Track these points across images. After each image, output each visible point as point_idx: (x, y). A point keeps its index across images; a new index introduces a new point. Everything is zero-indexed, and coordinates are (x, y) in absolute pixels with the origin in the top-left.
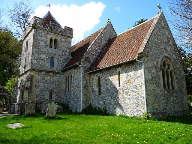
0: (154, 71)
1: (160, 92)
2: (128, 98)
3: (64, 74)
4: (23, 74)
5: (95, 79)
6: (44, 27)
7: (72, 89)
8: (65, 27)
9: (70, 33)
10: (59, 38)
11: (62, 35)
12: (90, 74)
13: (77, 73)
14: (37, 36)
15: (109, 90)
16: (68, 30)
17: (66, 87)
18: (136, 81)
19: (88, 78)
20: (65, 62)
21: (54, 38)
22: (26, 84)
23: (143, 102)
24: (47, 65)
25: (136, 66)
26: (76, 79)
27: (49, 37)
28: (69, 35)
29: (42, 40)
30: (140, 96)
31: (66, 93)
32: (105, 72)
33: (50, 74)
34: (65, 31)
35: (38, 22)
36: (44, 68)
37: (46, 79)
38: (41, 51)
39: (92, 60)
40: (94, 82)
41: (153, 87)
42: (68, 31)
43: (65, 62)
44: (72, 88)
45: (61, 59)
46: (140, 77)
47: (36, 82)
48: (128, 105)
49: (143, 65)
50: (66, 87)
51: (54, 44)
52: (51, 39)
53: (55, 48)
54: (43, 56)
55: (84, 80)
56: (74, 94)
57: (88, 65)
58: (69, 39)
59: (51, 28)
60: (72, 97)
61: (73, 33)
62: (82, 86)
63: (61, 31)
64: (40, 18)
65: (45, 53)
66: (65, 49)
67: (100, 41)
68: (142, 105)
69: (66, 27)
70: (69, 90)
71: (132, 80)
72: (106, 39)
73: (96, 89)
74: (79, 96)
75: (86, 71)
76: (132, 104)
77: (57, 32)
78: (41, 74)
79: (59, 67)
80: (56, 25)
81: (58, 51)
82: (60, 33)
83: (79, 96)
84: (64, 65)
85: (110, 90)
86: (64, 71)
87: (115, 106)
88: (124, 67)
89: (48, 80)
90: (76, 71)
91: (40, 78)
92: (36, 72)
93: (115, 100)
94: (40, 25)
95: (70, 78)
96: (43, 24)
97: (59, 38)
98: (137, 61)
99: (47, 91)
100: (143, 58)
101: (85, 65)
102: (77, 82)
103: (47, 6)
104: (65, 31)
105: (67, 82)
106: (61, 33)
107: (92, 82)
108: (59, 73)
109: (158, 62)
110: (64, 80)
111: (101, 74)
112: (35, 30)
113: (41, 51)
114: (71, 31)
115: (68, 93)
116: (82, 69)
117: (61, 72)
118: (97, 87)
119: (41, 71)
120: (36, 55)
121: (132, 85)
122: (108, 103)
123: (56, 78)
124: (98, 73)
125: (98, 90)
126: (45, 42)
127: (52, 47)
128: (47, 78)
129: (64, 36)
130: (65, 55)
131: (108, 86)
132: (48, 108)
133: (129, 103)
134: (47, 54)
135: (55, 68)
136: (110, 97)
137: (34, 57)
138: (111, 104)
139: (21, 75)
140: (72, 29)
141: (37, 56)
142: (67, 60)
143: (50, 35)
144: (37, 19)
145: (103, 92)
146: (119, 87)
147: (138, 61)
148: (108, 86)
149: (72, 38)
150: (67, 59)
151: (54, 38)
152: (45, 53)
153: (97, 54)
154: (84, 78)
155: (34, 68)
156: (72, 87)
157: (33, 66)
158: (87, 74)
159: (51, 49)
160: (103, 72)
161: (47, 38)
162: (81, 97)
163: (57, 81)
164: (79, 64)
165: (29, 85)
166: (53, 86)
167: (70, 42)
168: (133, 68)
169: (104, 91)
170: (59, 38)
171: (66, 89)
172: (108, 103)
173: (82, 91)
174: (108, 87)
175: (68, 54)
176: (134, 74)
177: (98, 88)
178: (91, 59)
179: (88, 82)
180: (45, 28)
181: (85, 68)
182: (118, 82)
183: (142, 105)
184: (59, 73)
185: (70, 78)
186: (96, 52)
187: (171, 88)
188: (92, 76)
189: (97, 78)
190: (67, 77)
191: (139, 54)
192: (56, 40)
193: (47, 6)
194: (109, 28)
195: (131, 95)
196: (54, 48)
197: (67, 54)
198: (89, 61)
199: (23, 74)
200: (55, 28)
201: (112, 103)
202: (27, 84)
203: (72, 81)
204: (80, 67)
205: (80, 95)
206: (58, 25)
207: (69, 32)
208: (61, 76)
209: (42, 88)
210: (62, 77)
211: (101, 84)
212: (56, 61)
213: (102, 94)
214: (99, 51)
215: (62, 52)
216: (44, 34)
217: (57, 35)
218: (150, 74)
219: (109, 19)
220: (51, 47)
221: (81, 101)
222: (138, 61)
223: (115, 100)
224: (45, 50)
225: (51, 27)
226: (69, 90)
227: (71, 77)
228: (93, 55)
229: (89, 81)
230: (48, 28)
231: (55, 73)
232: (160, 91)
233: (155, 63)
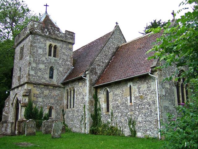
0: (168, 86)
1: (174, 109)
2: (140, 115)
4: (18, 87)
9: (71, 39)
10: (58, 45)
11: (62, 41)
13: (81, 87)
14: (35, 43)
15: (118, 106)
16: (69, 35)
18: (149, 97)
20: (66, 73)
21: (54, 44)
22: (24, 100)
23: (156, 120)
24: (47, 77)
25: (149, 81)
27: (48, 43)
28: (71, 41)
29: (40, 48)
30: (153, 113)
33: (49, 87)
36: (43, 81)
37: (44, 94)
38: (39, 60)
41: (167, 104)
42: (69, 36)
43: (66, 73)
44: (75, 104)
46: (153, 93)
47: (34, 97)
48: (140, 123)
51: (53, 51)
52: (50, 46)
54: (42, 66)
55: (90, 94)
56: (77, 111)
57: (95, 77)
58: (70, 46)
59: (50, 33)
63: (61, 36)
65: (43, 63)
66: (65, 57)
70: (72, 107)
75: (91, 84)
76: (144, 123)
77: (57, 38)
78: (39, 88)
79: (58, 79)
80: (56, 29)
84: (65, 77)
85: (120, 107)
86: (65, 84)
88: (136, 81)
89: (47, 94)
90: (80, 84)
91: (38, 92)
92: (34, 85)
94: (38, 30)
95: (72, 92)
96: (41, 29)
97: (59, 44)
98: (150, 75)
99: (46, 107)
100: (156, 73)
101: (91, 77)
102: (82, 96)
103: (44, 5)
104: (66, 36)
105: (69, 97)
106: (62, 39)
108: (60, 87)
110: (65, 95)
111: (109, 88)
112: (33, 36)
114: (72, 36)
115: (70, 109)
116: (88, 82)
119: (40, 84)
120: (34, 65)
121: (144, 101)
123: (56, 92)
124: (106, 87)
126: (44, 49)
127: (51, 56)
128: (46, 92)
129: (65, 42)
130: (66, 65)
131: (117, 102)
132: (54, 126)
133: (141, 121)
134: (45, 63)
135: (55, 81)
136: (120, 115)
137: (32, 68)
138: (121, 122)
139: (15, 88)
140: (73, 33)
141: (35, 66)
145: (111, 108)
146: (131, 104)
148: (117, 102)
149: (73, 44)
151: (54, 44)
154: (90, 93)
155: (32, 80)
156: (75, 103)
157: (31, 78)
160: (112, 86)
161: (45, 46)
164: (84, 76)
165: (27, 100)
166: (52, 101)
167: (71, 49)
168: (145, 83)
169: (113, 107)
171: (67, 105)
174: (118, 104)
175: (70, 64)
178: (97, 70)
180: (44, 33)
181: (91, 80)
182: (129, 98)
183: (155, 123)
184: (60, 87)
185: (72, 92)
186: (103, 63)
189: (105, 93)
190: (69, 91)
191: (152, 68)
192: (55, 47)
193: (44, 5)
196: (54, 56)
197: (69, 63)
198: (96, 73)
199: (18, 87)
200: (54, 33)
202: (25, 99)
203: (75, 96)
206: (58, 29)
208: (62, 89)
209: (41, 104)
211: (110, 99)
213: (110, 111)
214: (107, 61)
216: (42, 40)
218: (163, 90)
219: (117, 23)
220: (50, 55)
225: (50, 31)
226: (72, 107)
227: (74, 91)
228: (100, 65)
230: (46, 33)
231: (55, 87)
232: (174, 108)
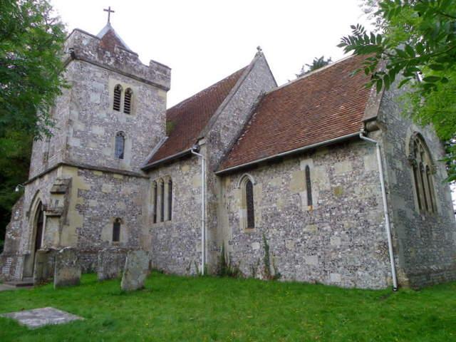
0: (399, 165)
1: (414, 217)
2: (336, 233)
3: (149, 178)
4: (41, 176)
5: (236, 191)
6: (101, 57)
7: (172, 215)
8: (151, 63)
9: (163, 78)
10: (136, 88)
11: (143, 81)
12: (223, 176)
13: (187, 174)
14: (82, 78)
15: (278, 214)
16: (158, 69)
17: (155, 210)
18: (358, 191)
19: (217, 184)
20: (152, 147)
21: (125, 86)
22: (54, 202)
23: (380, 242)
24: (109, 154)
25: (356, 153)
26: (184, 190)
27: (113, 82)
28: (162, 83)
29: (95, 91)
30: (371, 228)
31: (154, 225)
32: (266, 169)
33: (115, 176)
34: (151, 72)
35: (85, 42)
36: (101, 162)
37: (103, 190)
38: (92, 117)
39: (227, 143)
40: (235, 197)
41: (402, 205)
42: (157, 72)
43: (152, 147)
44: (173, 213)
45: (141, 139)
46: (369, 179)
47: (79, 196)
48: (335, 250)
49: (378, 150)
50: (155, 210)
51: (123, 101)
52: (118, 90)
53: (127, 111)
54: (98, 130)
55: (208, 190)
56: (179, 228)
57: (218, 154)
58: (160, 93)
59: (117, 62)
60: (175, 235)
61: (170, 79)
62: (203, 206)
63: (141, 72)
64: (91, 35)
65: (101, 123)
66: (150, 116)
67: (242, 97)
68: (379, 251)
69: (155, 62)
70: (166, 217)
71: (345, 187)
72: (254, 93)
73: (242, 214)
74: (193, 230)
75: (212, 169)
76: (349, 250)
77: (133, 74)
78: (92, 177)
79: (136, 160)
80: (130, 54)
81: (135, 118)
82: (139, 76)
83: (193, 230)
84: (150, 156)
85: (282, 215)
86: (149, 170)
87: (297, 255)
88: (323, 156)
89: (110, 191)
90: (186, 168)
91: (88, 187)
92: (80, 171)
93: (299, 240)
94: (90, 52)
95: (166, 186)
96: (98, 51)
97: (137, 88)
98: (362, 140)
99: (108, 220)
100: (378, 133)
101: (212, 153)
102: (189, 195)
103: (105, 10)
104: (151, 72)
105: (159, 198)
106: (143, 77)
107: (227, 195)
108: (138, 176)
109: (404, 144)
110: (150, 193)
111: (253, 175)
112: (78, 63)
113: (92, 117)
114: (165, 72)
115: (162, 224)
116: (203, 164)
117: (141, 173)
118: (244, 208)
119: (92, 169)
120: (80, 127)
121: (346, 200)
122: (276, 247)
123: (128, 188)
124: (246, 174)
125: (246, 215)
126: (104, 95)
127: (118, 110)
128: (108, 187)
129: (149, 83)
130: (150, 130)
131: (274, 205)
132: (128, 263)
133: (338, 247)
134: (107, 124)
135: (127, 164)
136: (282, 233)
137: (75, 133)
138: (286, 250)
139: (35, 179)
140: (166, 67)
141: (83, 130)
142: (156, 141)
143: (115, 78)
144: (83, 35)
145: (260, 220)
146: (310, 207)
147: (364, 138)
148: (274, 205)
149: (167, 89)
150: (156, 141)
151: (125, 86)
152: (101, 123)
153: (237, 129)
154: (208, 186)
155: (75, 158)
156: (173, 209)
157: (71, 154)
158: (215, 176)
159: (116, 112)
160: (261, 171)
161: (106, 87)
162: (200, 235)
163: (131, 196)
164: (195, 151)
165: (61, 203)
166: (121, 206)
167: (162, 100)
168: (347, 158)
169: (265, 217)
170: (136, 88)
171: (155, 217)
172: (276, 247)
173: (203, 219)
174: (275, 208)
175: (160, 129)
176: (350, 173)
177: (246, 210)
178: (223, 138)
179: (218, 196)
180: (102, 59)
181: (210, 160)
182: (304, 194)
183: (379, 251)
184: (138, 176)
185: (166, 186)
186: (234, 123)
187: (430, 210)
188: (228, 181)
189: (243, 186)
190: (159, 184)
191: (365, 122)
192: (128, 93)
193: (105, 10)
194: (262, 68)
195: (346, 224)
196: (125, 112)
197: (157, 127)
198: (220, 144)
199: (41, 176)
200: (126, 63)
201: (290, 245)
202: (57, 202)
203: (173, 194)
204: (197, 158)
205: (198, 229)
206: (135, 56)
207: (158, 77)
208: (143, 182)
209: (95, 211)
210: (145, 189)
211: (257, 198)
212: (129, 145)
213: (256, 225)
214: (242, 122)
215: (145, 123)
216: (99, 75)
217: (131, 80)
218: (394, 173)
219: (258, 48)
220: (116, 108)
221: (200, 244)
222: (364, 138)
223: (299, 240)
224: (103, 114)
225: (116, 58)
226: (166, 217)
227: (170, 183)
228: (228, 129)
229: (221, 193)
230: (109, 60)
231: (127, 175)
232: (414, 215)
233: (399, 146)
